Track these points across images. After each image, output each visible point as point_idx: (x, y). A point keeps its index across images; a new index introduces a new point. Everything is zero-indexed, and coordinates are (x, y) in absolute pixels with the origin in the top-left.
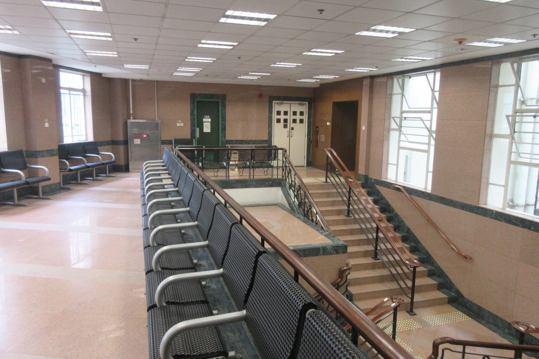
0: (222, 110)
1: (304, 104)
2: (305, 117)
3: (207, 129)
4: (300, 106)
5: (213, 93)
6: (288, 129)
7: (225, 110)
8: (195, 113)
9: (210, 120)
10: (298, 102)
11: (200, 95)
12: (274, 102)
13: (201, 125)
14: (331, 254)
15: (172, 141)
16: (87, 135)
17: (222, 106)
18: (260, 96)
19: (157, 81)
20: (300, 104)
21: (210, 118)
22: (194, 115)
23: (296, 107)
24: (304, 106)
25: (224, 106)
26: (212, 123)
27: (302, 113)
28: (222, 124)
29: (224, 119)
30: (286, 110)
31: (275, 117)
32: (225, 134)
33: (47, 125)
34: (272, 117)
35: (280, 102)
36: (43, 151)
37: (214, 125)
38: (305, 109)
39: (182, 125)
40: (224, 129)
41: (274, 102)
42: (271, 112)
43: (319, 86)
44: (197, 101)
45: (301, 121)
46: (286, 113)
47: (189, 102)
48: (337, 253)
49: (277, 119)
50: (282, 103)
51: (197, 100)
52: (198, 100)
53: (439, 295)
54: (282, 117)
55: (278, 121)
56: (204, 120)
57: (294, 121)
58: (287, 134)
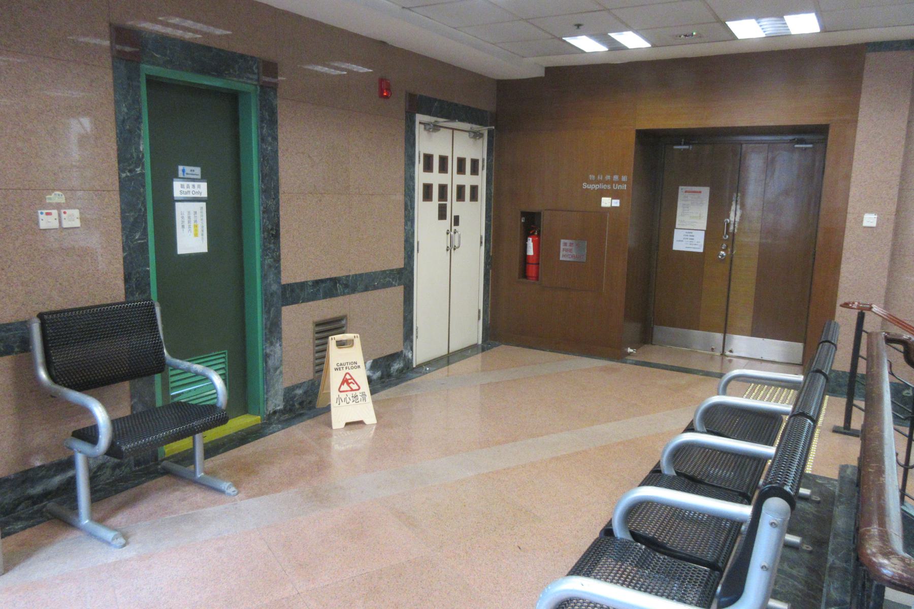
0: (262, 139)
2: (480, 180)
3: (192, 238)
6: (446, 224)
7: (275, 138)
8: (144, 146)
9: (202, 189)
10: (466, 126)
12: (419, 118)
15: (24, 325)
17: (262, 120)
20: (476, 135)
21: (204, 178)
22: (140, 162)
24: (480, 141)
25: (270, 120)
26: (210, 201)
28: (266, 211)
29: (271, 189)
31: (421, 177)
32: (278, 260)
37: (226, 216)
39: (72, 218)
40: (273, 235)
41: (419, 118)
43: (541, 73)
44: (152, 82)
47: (106, 78)
50: (436, 128)
51: (147, 69)
56: (179, 188)
58: (444, 241)
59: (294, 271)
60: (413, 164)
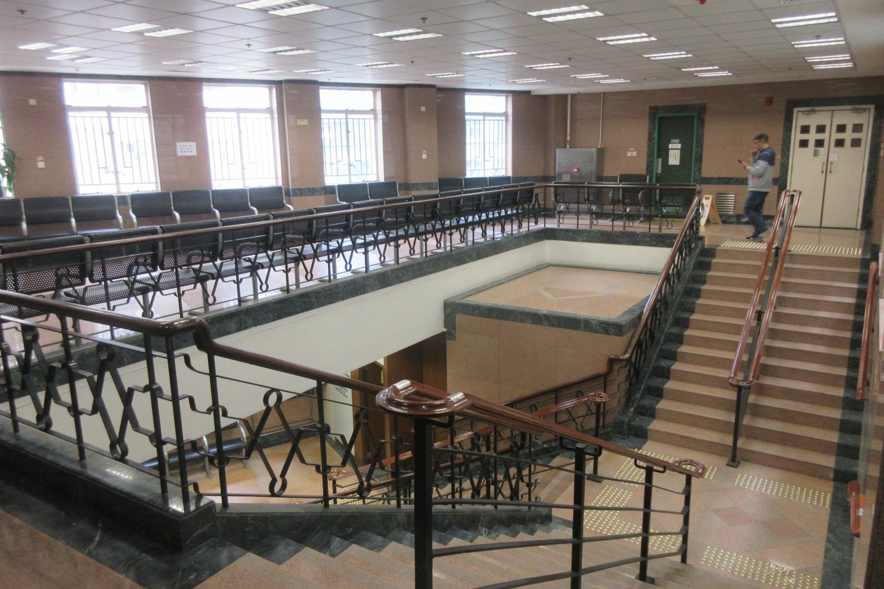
0: (697, 129)
1: (865, 110)
2: (866, 136)
3: (674, 159)
4: (854, 114)
5: (684, 103)
7: (703, 128)
8: (656, 135)
9: (679, 146)
10: (850, 107)
11: (663, 108)
13: (664, 153)
14: (597, 332)
16: (506, 169)
18: (769, 101)
19: (604, 93)
20: (855, 110)
22: (654, 139)
23: (846, 116)
25: (702, 122)
26: (682, 150)
27: (857, 128)
29: (700, 144)
30: (821, 123)
31: (796, 136)
32: (700, 169)
33: (424, 156)
34: (789, 137)
35: (809, 108)
36: (417, 184)
38: (867, 118)
39: (635, 154)
40: (699, 159)
42: (788, 129)
45: (856, 143)
46: (821, 129)
48: (607, 332)
49: (860, 140)
50: (814, 111)
52: (661, 115)
53: (829, 461)
54: (812, 136)
55: (804, 144)
56: (670, 146)
57: (840, 143)
59: (706, 172)
60: (790, 131)
